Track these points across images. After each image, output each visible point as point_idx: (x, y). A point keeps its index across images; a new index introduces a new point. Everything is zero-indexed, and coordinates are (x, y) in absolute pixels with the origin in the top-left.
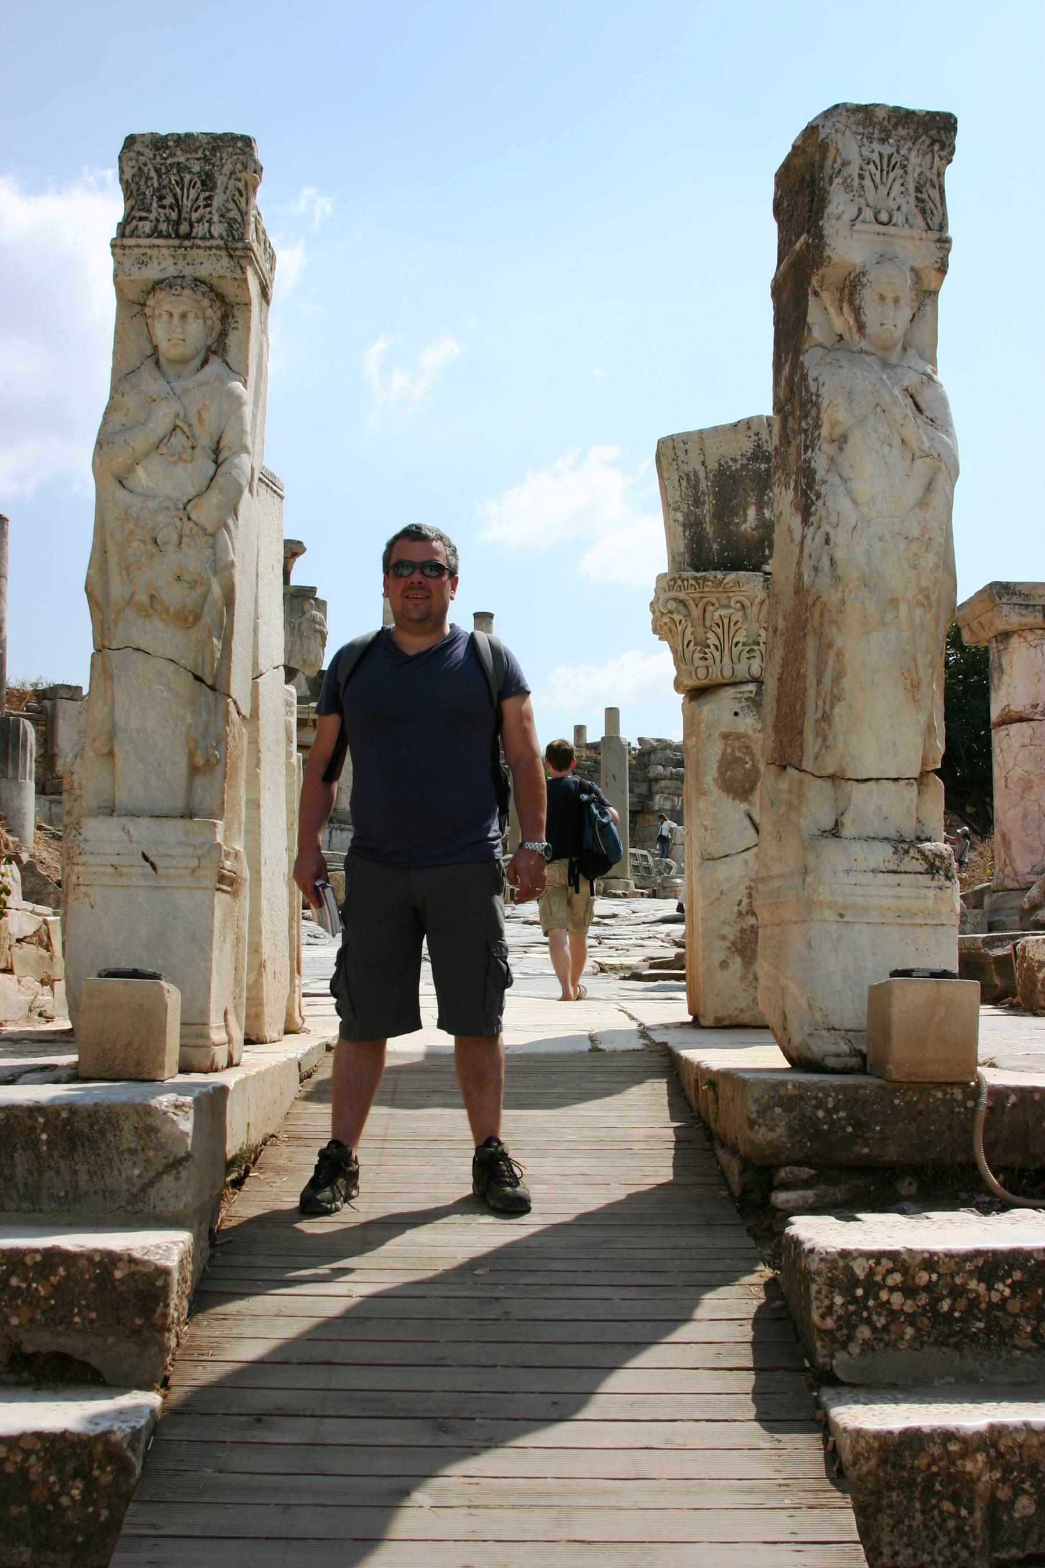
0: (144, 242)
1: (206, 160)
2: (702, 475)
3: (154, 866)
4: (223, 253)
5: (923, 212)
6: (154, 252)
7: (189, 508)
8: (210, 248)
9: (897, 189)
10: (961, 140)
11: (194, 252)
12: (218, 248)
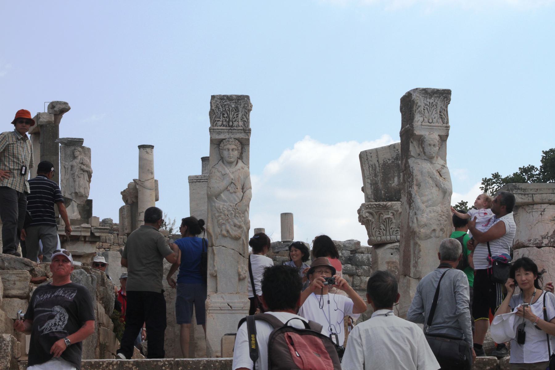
0: (219, 128)
2: (377, 165)
5: (442, 118)
9: (434, 112)
10: (452, 97)
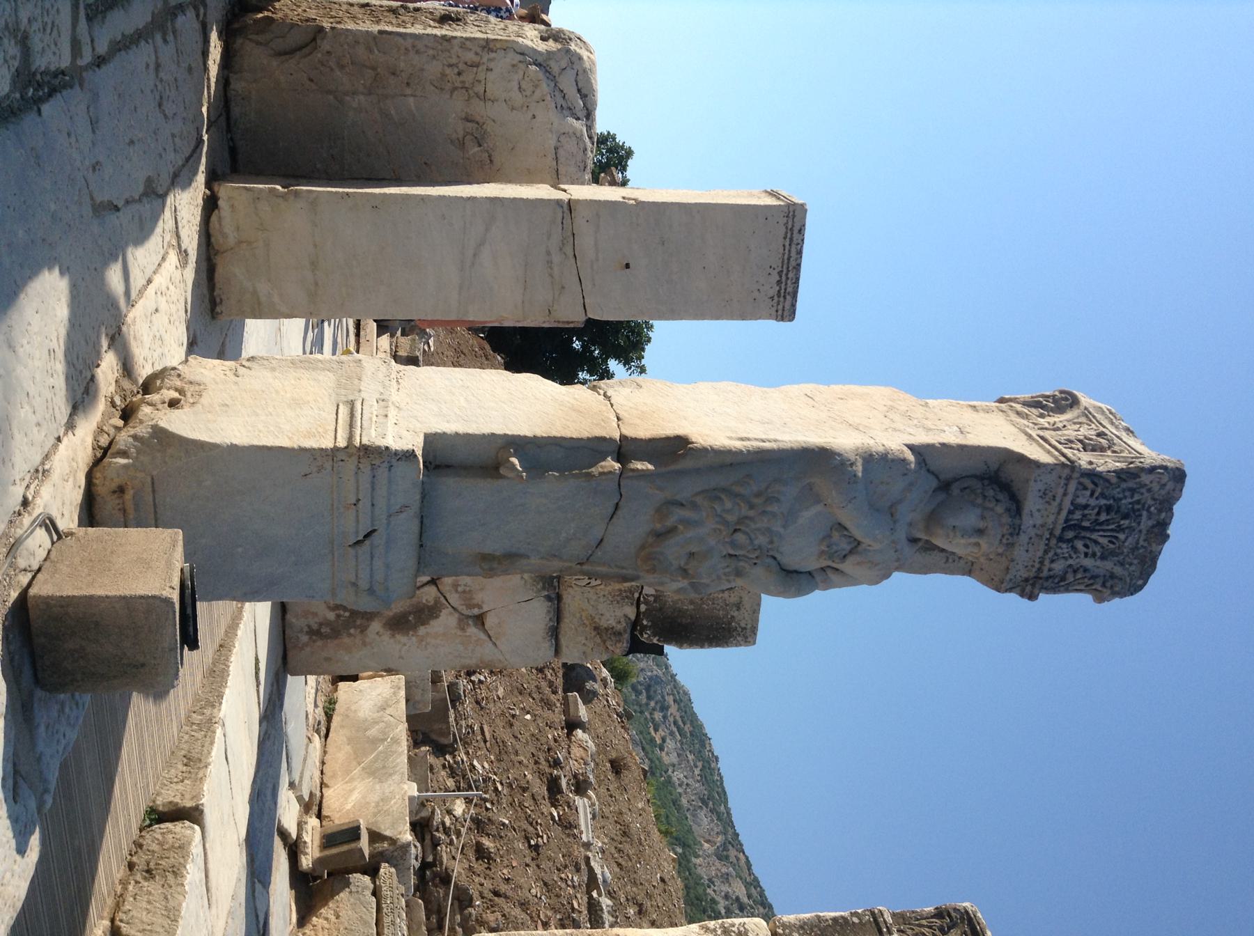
1: (1135, 549)
3: (358, 543)
4: (1032, 574)
6: (1054, 506)
7: (769, 560)
8: (1042, 563)
11: (1042, 547)
12: (1040, 570)
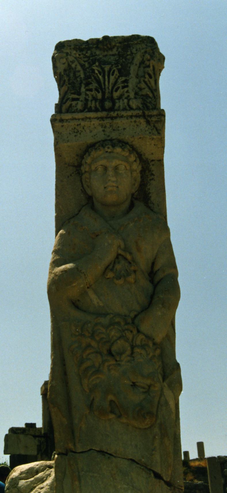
4: (142, 120)
7: (136, 321)
8: (131, 117)
12: (137, 116)
